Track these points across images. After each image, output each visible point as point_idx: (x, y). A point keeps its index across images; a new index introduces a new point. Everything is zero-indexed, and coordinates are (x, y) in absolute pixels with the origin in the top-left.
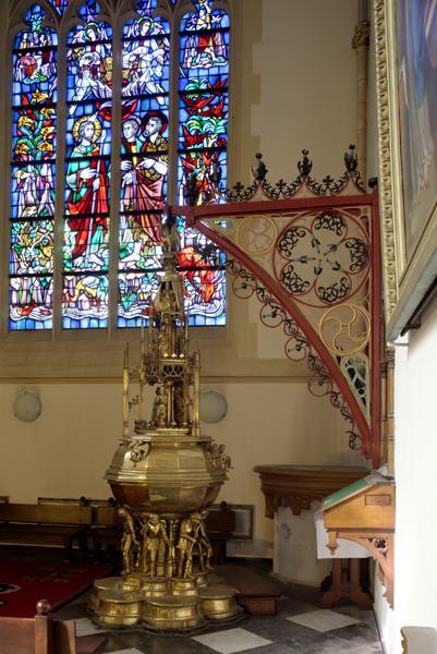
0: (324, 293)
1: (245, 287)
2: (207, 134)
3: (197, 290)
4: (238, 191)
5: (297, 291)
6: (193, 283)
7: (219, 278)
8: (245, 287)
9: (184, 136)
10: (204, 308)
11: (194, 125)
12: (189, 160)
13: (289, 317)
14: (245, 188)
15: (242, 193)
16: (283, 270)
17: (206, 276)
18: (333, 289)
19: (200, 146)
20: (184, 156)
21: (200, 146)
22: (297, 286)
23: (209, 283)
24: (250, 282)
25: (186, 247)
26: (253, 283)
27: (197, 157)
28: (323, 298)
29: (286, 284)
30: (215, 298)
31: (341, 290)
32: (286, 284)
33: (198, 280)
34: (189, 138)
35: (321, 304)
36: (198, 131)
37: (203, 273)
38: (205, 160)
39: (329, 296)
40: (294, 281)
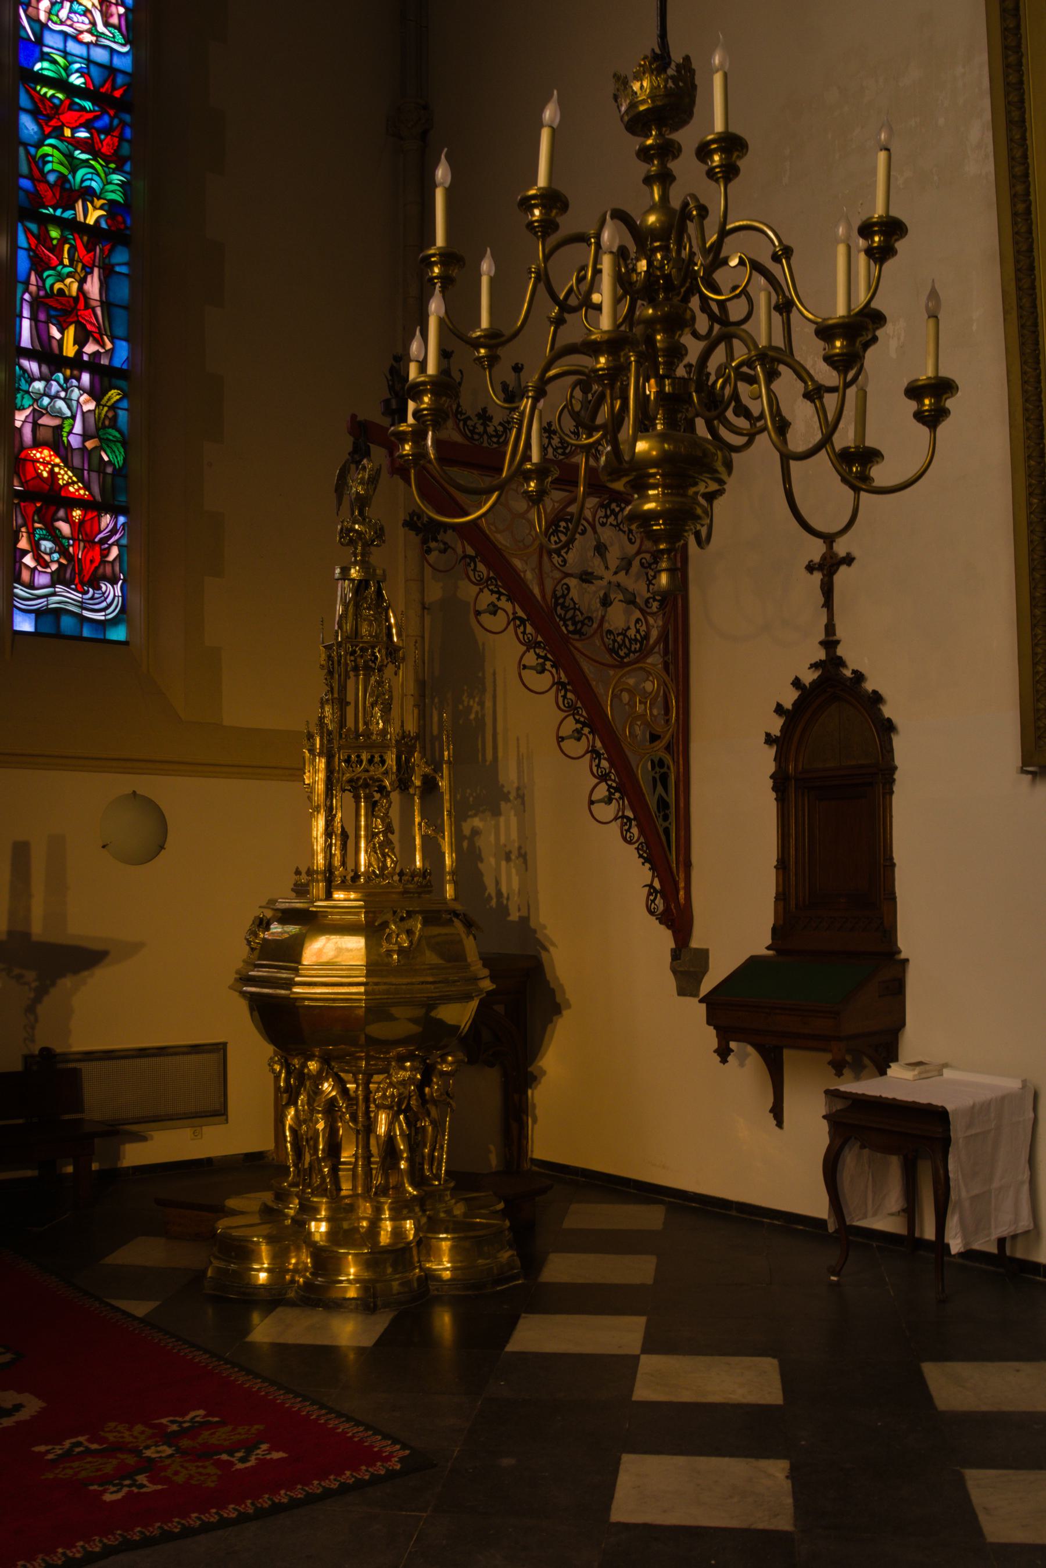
0: (614, 641)
1: (494, 613)
2: (87, 194)
3: (63, 551)
4: (485, 425)
5: (574, 632)
6: (55, 536)
7: (114, 532)
8: (494, 613)
9: (30, 177)
10: (78, 596)
11: (55, 164)
12: (43, 238)
13: (564, 679)
14: (496, 422)
15: (490, 430)
16: (555, 591)
17: (82, 522)
18: (625, 635)
19: (68, 214)
20: (33, 227)
21: (68, 214)
22: (575, 624)
23: (90, 542)
24: (504, 603)
25: (37, 444)
26: (508, 606)
27: (63, 240)
28: (612, 651)
29: (560, 616)
30: (105, 578)
31: (636, 640)
32: (560, 616)
33: (65, 528)
34: (42, 187)
35: (607, 659)
36: (62, 178)
37: (77, 513)
38: (81, 251)
39: (620, 647)
40: (570, 614)
